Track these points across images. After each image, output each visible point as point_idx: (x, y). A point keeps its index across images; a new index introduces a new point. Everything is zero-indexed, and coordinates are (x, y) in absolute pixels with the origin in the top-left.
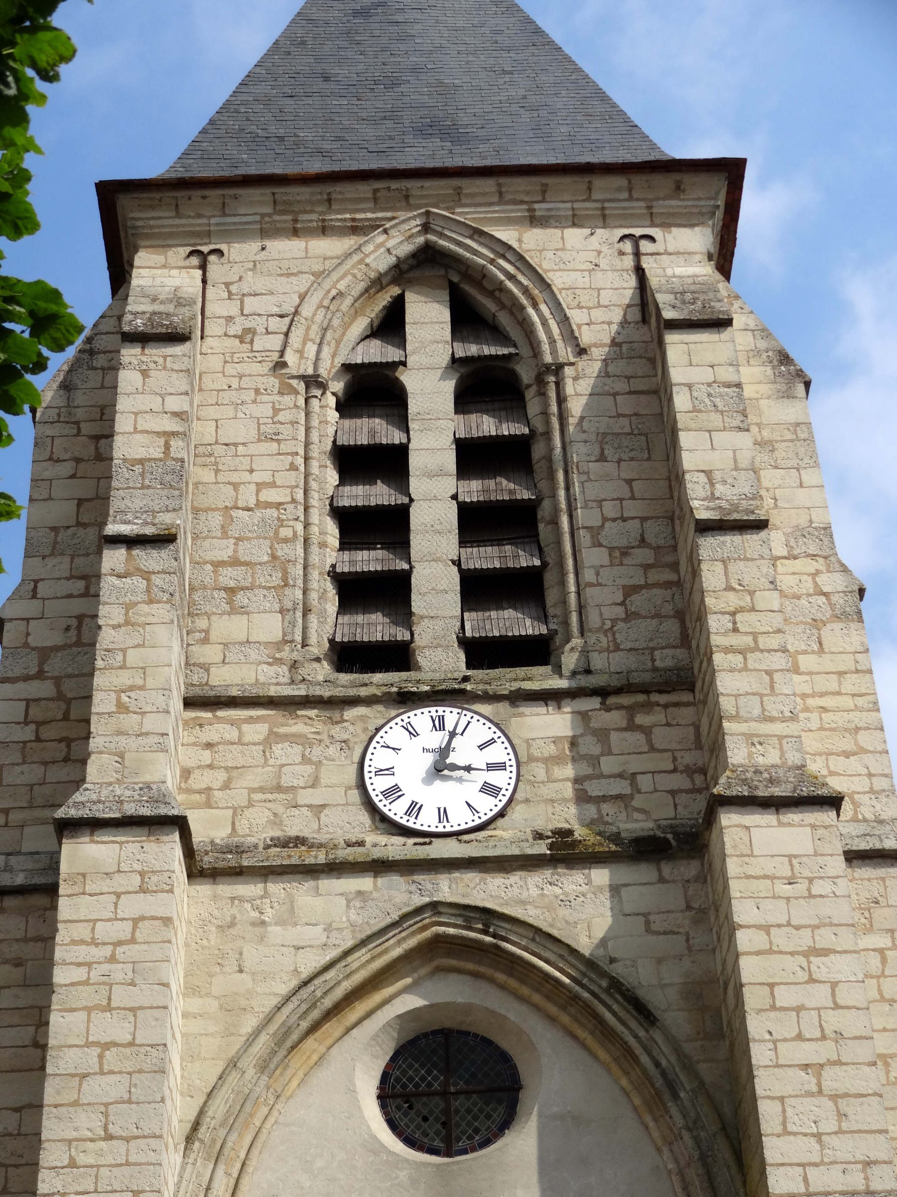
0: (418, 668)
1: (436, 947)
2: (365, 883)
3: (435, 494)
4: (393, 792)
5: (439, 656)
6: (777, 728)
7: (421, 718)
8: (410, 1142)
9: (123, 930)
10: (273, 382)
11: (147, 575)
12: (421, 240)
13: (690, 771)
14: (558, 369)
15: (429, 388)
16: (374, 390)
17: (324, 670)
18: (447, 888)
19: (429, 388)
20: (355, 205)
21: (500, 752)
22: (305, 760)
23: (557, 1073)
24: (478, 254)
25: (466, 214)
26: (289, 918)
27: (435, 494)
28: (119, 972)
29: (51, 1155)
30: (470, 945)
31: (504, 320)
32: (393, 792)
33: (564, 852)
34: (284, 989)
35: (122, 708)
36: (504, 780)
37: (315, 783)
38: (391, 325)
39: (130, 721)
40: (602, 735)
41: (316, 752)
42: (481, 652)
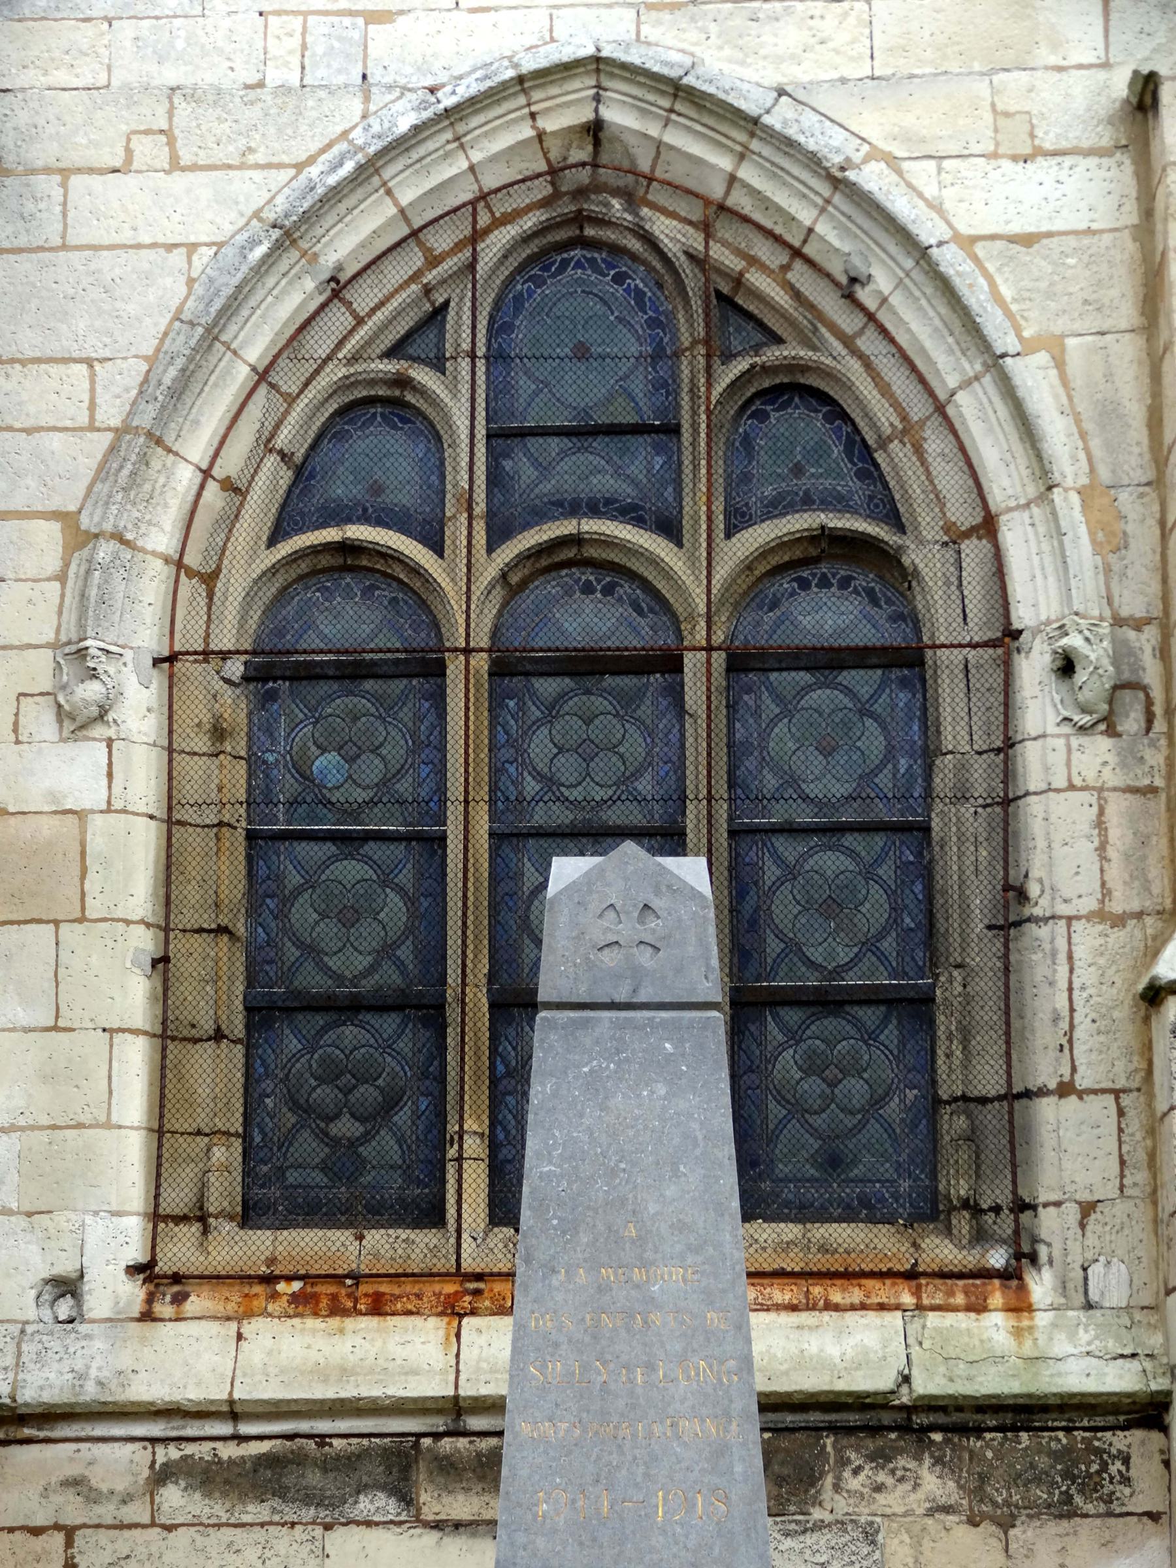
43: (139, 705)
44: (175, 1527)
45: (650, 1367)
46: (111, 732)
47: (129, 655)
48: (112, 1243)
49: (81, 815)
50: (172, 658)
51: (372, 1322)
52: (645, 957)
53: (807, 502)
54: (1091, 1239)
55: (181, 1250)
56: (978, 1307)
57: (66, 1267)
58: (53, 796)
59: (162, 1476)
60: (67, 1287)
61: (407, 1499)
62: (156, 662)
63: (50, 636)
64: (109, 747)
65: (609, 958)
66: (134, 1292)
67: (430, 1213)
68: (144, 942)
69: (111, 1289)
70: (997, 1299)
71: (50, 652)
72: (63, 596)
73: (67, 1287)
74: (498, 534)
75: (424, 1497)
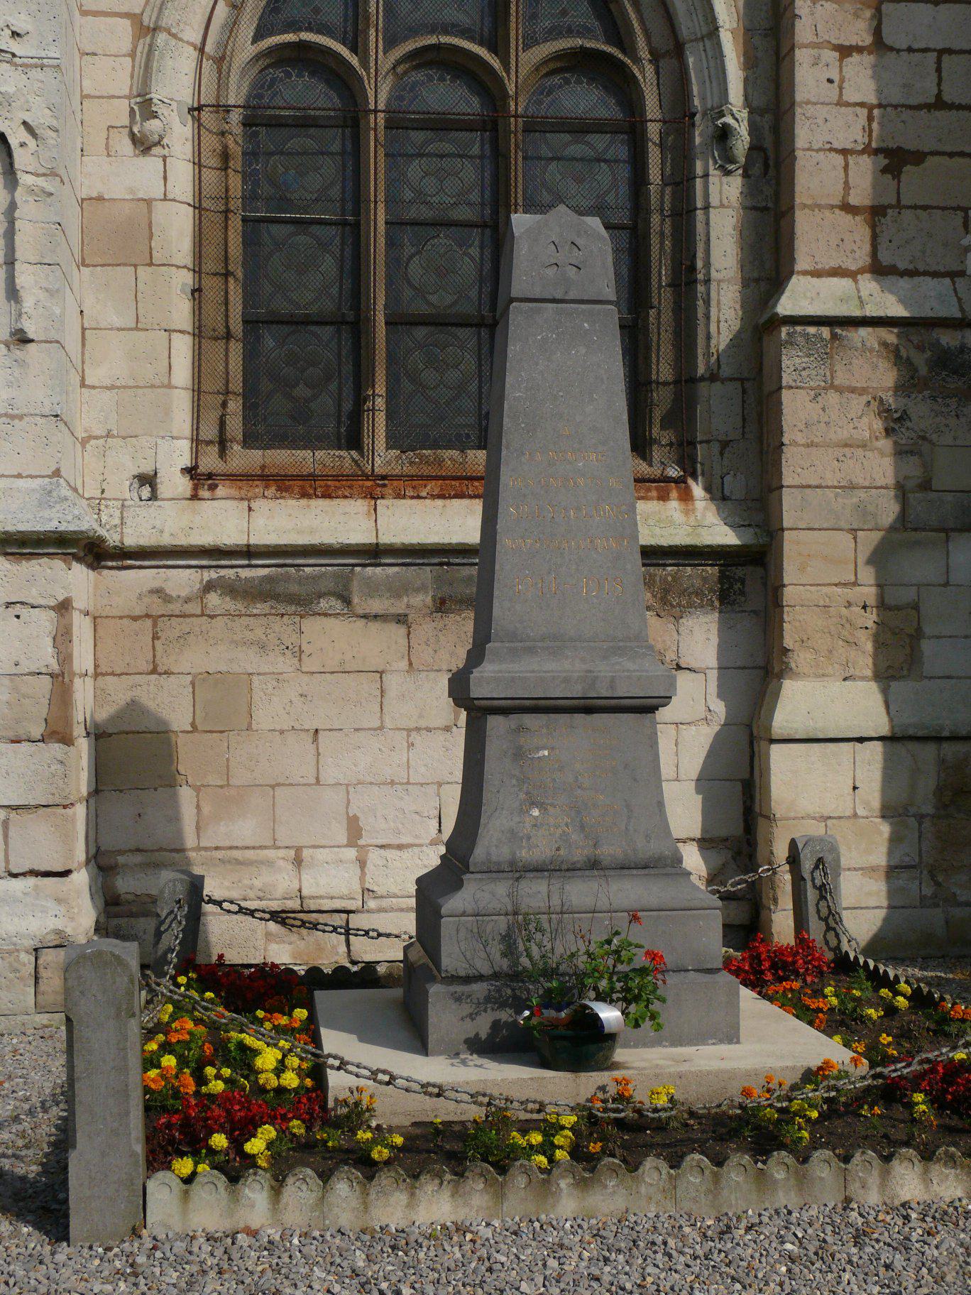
43: (179, 136)
44: (215, 616)
45: (578, 509)
46: (166, 152)
47: (174, 105)
48: (174, 456)
49: (149, 202)
50: (199, 109)
51: (327, 502)
52: (572, 272)
53: (570, 32)
54: (726, 462)
55: (210, 461)
56: (663, 497)
57: (147, 468)
58: (132, 191)
59: (209, 587)
60: (148, 480)
61: (347, 601)
62: (191, 110)
63: (127, 92)
64: (164, 161)
65: (551, 272)
66: (183, 485)
67: (354, 440)
68: (187, 278)
69: (174, 483)
70: (674, 494)
71: (127, 101)
72: (133, 67)
73: (148, 480)
74: (391, 43)
75: (356, 600)
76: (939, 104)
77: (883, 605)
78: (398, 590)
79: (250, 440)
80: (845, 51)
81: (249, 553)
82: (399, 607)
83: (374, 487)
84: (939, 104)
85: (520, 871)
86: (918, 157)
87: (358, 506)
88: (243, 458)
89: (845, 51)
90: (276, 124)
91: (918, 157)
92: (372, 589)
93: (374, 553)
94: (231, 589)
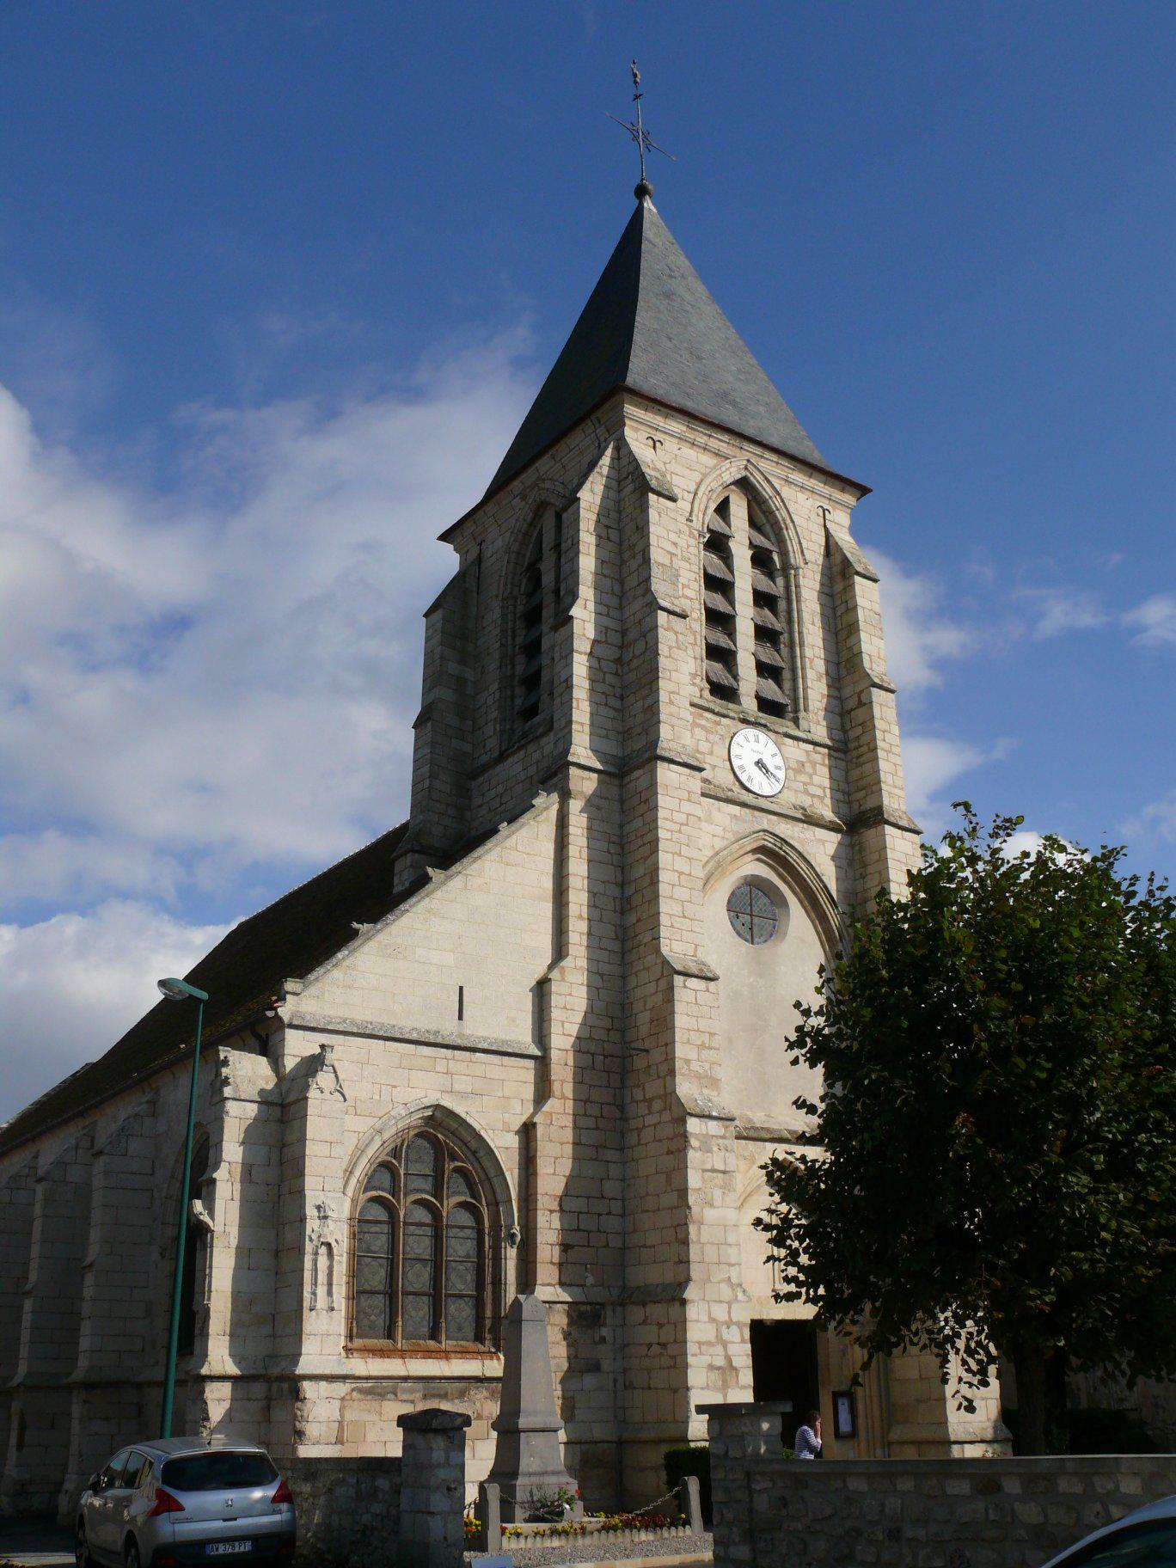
0: (739, 704)
1: (762, 850)
2: (736, 809)
3: (746, 615)
4: (742, 767)
5: (749, 704)
6: (897, 792)
7: (751, 732)
8: (738, 934)
9: (682, 818)
10: (686, 529)
11: (676, 633)
12: (744, 473)
13: (844, 793)
14: (797, 569)
15: (741, 553)
16: (717, 544)
17: (707, 693)
18: (767, 822)
19: (741, 553)
20: (719, 442)
21: (779, 761)
22: (707, 740)
23: (799, 921)
24: (766, 491)
25: (762, 464)
26: (709, 821)
27: (746, 615)
28: (684, 839)
29: (664, 919)
30: (776, 855)
31: (768, 528)
32: (742, 767)
33: (811, 820)
34: (709, 853)
35: (671, 702)
36: (781, 774)
37: (711, 753)
38: (723, 509)
39: (673, 709)
40: (814, 764)
41: (711, 737)
42: (767, 706)
67: (390, 1335)
74: (405, 1195)
76: (578, 1230)
77: (564, 1398)
78: (412, 1391)
79: (360, 1336)
80: (552, 1211)
81: (368, 1378)
82: (411, 1397)
83: (403, 1354)
84: (578, 1230)
85: (530, 1474)
86: (572, 1247)
87: (399, 1361)
88: (358, 1343)
89: (552, 1211)
90: (368, 1221)
91: (572, 1247)
92: (404, 1391)
93: (405, 1379)
94: (360, 1391)
